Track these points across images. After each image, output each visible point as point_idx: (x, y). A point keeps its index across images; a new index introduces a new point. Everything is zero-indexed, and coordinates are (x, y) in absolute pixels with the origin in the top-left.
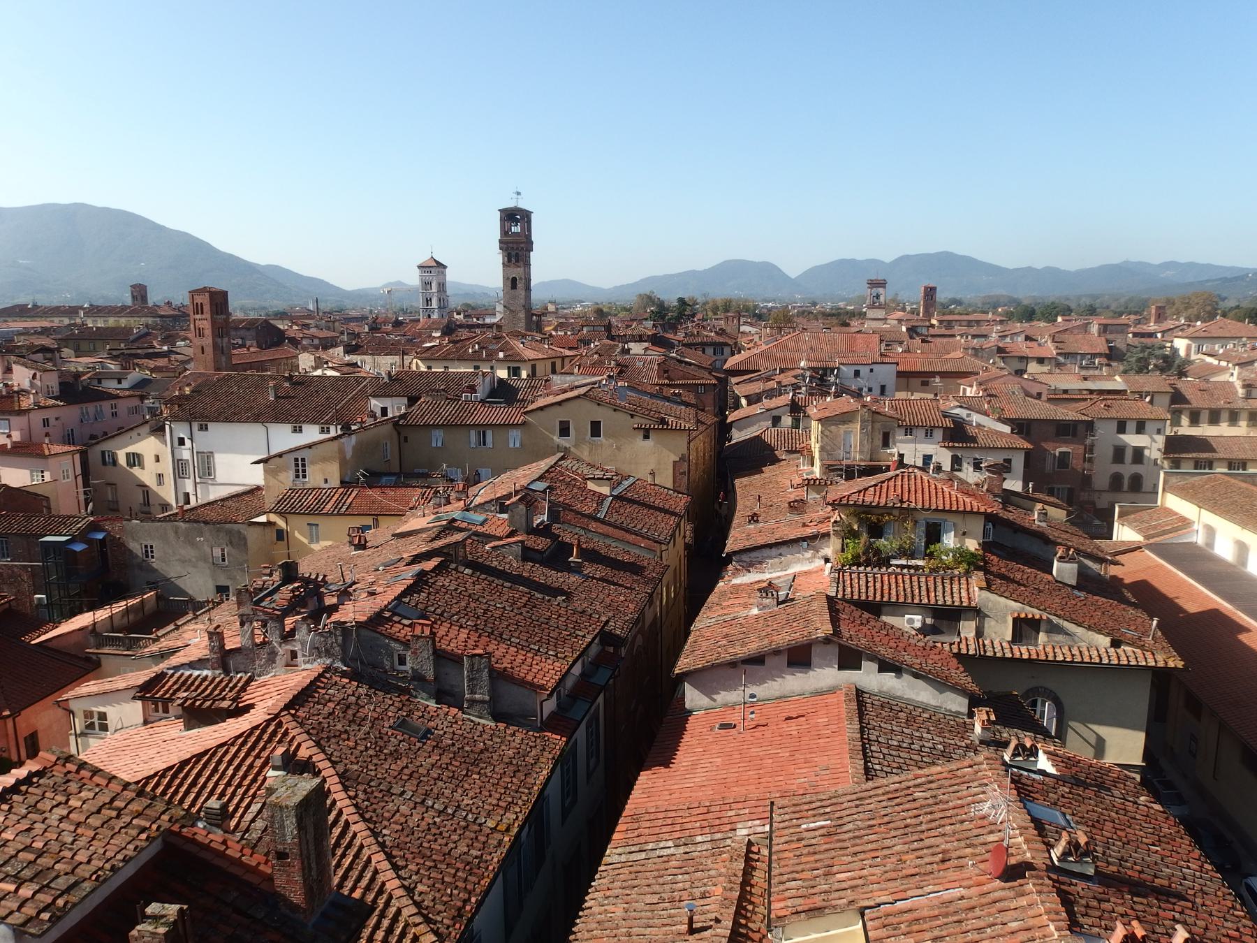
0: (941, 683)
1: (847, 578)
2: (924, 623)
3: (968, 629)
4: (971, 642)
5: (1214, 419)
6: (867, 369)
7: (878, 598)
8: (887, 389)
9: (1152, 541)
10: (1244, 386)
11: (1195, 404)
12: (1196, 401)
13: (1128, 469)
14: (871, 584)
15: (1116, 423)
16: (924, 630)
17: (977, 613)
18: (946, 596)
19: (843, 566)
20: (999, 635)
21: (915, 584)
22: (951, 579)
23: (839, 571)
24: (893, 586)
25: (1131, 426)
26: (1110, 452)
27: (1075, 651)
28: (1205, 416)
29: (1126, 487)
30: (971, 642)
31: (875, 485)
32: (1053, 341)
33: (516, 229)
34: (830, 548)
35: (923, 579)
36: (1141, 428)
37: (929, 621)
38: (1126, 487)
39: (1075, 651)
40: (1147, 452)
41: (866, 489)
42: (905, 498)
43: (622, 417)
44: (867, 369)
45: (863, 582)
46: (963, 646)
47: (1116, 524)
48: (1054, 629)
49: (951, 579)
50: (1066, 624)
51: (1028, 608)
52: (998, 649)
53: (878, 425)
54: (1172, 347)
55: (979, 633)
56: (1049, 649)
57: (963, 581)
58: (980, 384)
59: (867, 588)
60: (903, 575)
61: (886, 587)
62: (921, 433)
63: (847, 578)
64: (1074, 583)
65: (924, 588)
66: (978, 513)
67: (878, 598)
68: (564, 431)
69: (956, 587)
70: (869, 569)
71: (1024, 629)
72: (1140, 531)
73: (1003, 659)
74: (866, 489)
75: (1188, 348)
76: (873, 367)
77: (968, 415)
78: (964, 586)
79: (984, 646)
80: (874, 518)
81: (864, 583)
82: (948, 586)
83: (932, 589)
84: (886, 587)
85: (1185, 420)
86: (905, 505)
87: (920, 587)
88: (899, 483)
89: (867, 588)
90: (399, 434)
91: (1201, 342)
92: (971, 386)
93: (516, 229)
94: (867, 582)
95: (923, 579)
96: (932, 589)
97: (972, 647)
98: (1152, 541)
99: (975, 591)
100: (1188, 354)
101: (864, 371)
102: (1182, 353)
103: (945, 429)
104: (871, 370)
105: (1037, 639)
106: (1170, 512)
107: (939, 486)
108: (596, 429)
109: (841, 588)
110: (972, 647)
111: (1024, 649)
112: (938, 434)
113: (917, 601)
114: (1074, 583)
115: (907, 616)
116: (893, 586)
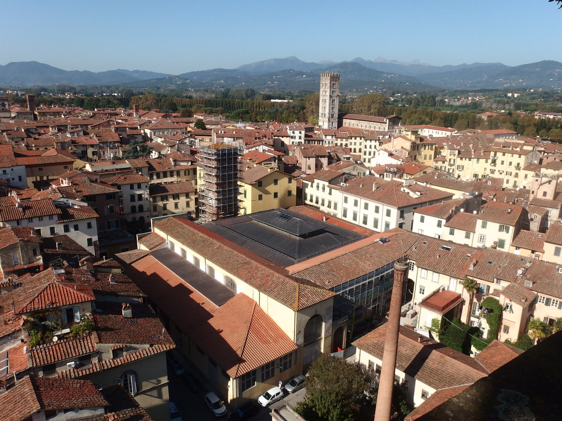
0: (93, 407)
1: (36, 353)
2: (76, 364)
3: (95, 360)
4: (97, 365)
5: (165, 176)
6: (10, 169)
7: (53, 361)
8: (22, 178)
9: (153, 250)
10: (173, 161)
11: (158, 170)
12: (158, 169)
13: (137, 203)
14: (48, 353)
15: (129, 186)
16: (77, 367)
17: (98, 353)
18: (83, 351)
19: (32, 347)
20: (108, 356)
21: (68, 346)
22: (83, 339)
23: (31, 351)
24: (58, 351)
25: (136, 186)
26: (129, 197)
27: (138, 354)
28: (162, 175)
29: (137, 211)
30: (97, 365)
31: (38, 296)
32: (96, 136)
34: (23, 335)
35: (71, 343)
36: (139, 187)
37: (78, 363)
38: (137, 211)
39: (138, 354)
40: (143, 196)
41: (34, 300)
42: (54, 302)
44: (10, 169)
45: (44, 354)
46: (94, 368)
47: (138, 243)
48: (128, 349)
49: (83, 339)
50: (133, 345)
51: (117, 344)
52: (109, 364)
53: (29, 247)
54: (144, 132)
55: (100, 360)
56: (128, 357)
57: (88, 338)
58: (70, 178)
59: (46, 356)
60: (61, 343)
61: (55, 353)
62: (46, 219)
63: (36, 353)
64: (131, 316)
65: (72, 348)
66: (88, 301)
67: (53, 361)
69: (86, 342)
70: (45, 345)
71: (116, 353)
72: (147, 246)
73: (112, 368)
74: (34, 300)
75: (151, 133)
76: (12, 168)
77: (67, 201)
78: (89, 341)
79: (103, 364)
80: (41, 315)
81: (44, 355)
82: (82, 343)
83: (76, 347)
84: (55, 353)
85: (155, 177)
86: (55, 306)
87: (70, 347)
88: (49, 292)
89: (46, 356)
91: (155, 131)
92: (65, 180)
94: (46, 353)
95: (71, 343)
96: (76, 347)
97: (98, 368)
98: (153, 250)
99: (93, 342)
100: (151, 136)
101: (8, 170)
102: (149, 135)
103: (58, 215)
104: (12, 170)
105: (122, 354)
106: (157, 235)
107: (68, 289)
109: (34, 361)
110: (98, 368)
111: (118, 360)
112: (56, 218)
113: (70, 356)
114: (131, 316)
115: (68, 364)
116: (58, 351)
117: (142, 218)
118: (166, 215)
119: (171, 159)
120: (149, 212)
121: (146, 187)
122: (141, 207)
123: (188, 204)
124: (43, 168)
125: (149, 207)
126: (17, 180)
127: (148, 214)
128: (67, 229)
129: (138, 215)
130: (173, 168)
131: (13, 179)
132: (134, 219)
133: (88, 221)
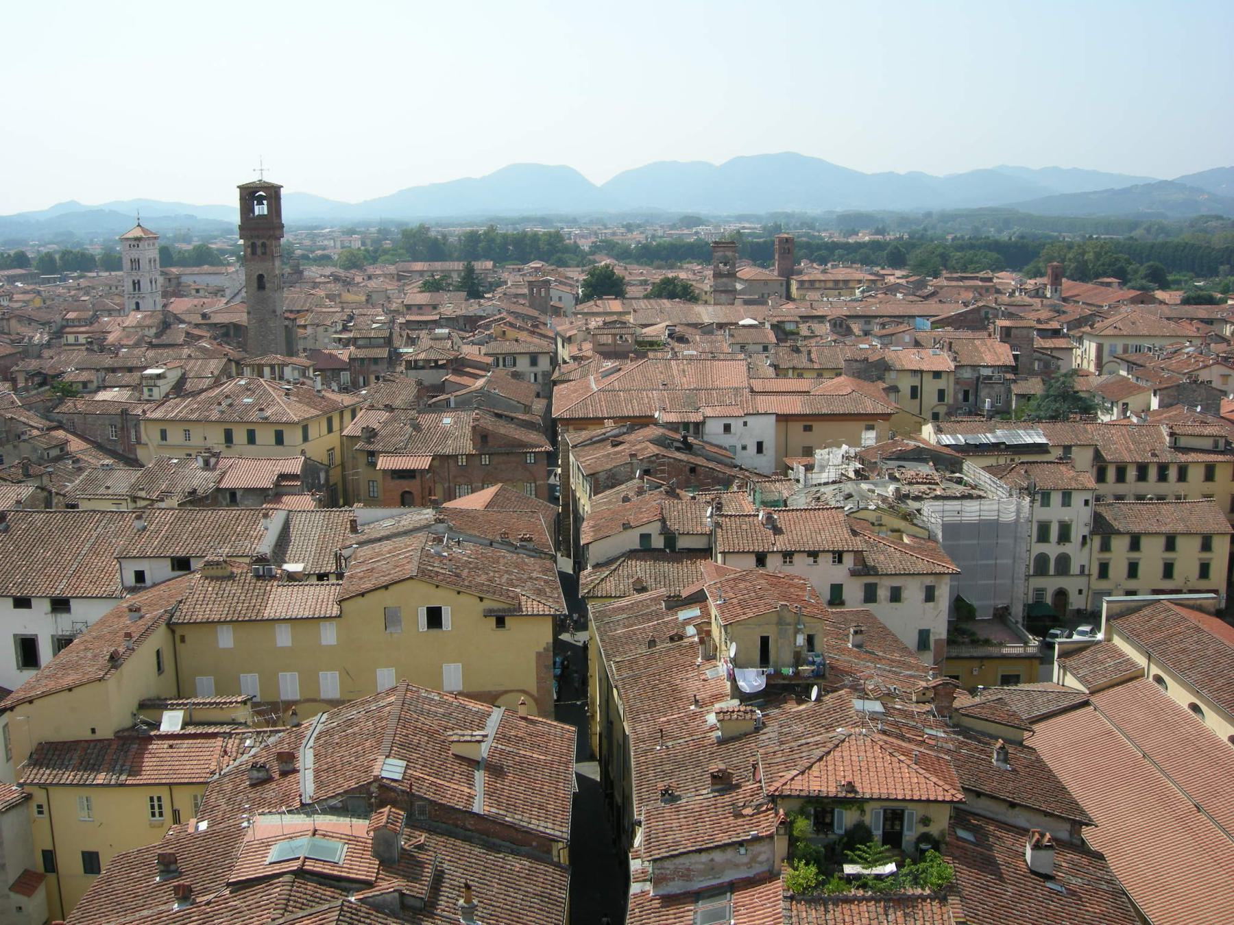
6: (741, 421)
13: (1052, 550)
25: (1056, 498)
29: (1052, 571)
33: (261, 210)
38: (1052, 571)
43: (469, 601)
44: (741, 421)
62: (825, 561)
66: (944, 801)
68: (391, 618)
72: (1082, 680)
90: (173, 632)
93: (261, 210)
101: (736, 425)
104: (745, 424)
108: (434, 617)
117: (1061, 594)
118: (1134, 593)
119: (1164, 431)
120: (1084, 580)
121: (1086, 503)
122: (1063, 563)
123: (1204, 571)
124: (816, 426)
125: (1085, 562)
126: (752, 449)
127: (1082, 582)
128: (870, 595)
129: (1051, 584)
130: (1167, 457)
131: (744, 448)
132: (1040, 592)
133: (929, 581)
